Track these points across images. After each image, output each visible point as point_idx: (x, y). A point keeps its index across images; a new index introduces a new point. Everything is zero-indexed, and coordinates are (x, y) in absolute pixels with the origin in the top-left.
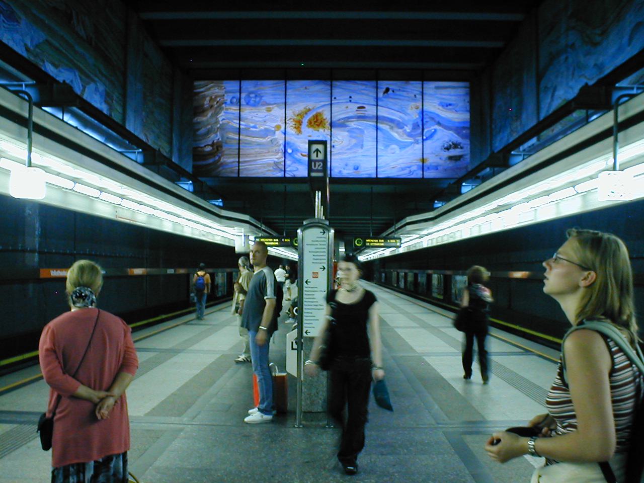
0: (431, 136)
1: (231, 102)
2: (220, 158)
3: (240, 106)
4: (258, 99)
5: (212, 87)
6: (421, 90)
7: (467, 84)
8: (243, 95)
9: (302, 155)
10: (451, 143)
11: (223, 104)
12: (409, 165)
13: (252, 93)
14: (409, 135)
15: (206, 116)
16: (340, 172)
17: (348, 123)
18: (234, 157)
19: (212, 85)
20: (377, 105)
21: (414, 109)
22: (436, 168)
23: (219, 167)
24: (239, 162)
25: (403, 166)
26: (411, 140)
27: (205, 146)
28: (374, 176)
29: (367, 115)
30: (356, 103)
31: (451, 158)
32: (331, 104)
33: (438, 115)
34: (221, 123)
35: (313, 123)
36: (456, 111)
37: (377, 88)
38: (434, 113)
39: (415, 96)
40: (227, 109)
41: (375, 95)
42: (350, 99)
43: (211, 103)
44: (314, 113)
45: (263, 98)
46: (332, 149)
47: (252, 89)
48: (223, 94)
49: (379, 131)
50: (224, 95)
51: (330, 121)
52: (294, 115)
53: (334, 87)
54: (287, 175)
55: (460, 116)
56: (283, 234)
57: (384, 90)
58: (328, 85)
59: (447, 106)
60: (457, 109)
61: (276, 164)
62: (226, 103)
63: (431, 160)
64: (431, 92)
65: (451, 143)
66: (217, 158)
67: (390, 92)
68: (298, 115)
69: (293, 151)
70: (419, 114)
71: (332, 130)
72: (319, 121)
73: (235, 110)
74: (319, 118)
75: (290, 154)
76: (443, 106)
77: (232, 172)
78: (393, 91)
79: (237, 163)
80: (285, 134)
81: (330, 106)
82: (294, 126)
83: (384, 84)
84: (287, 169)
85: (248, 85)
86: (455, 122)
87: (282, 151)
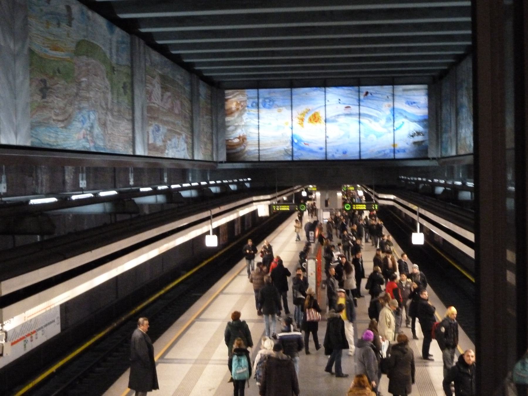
0: (400, 127)
1: (252, 106)
2: (245, 147)
3: (258, 108)
4: (271, 103)
5: (237, 95)
6: (392, 92)
7: (425, 86)
8: (261, 100)
9: (304, 144)
10: (415, 132)
11: (245, 107)
12: (384, 149)
13: (267, 98)
14: (385, 127)
15: (234, 116)
16: (333, 156)
17: (337, 119)
18: (256, 147)
19: (238, 93)
20: (359, 105)
21: (387, 107)
22: (404, 151)
23: (244, 154)
24: (259, 150)
25: (380, 150)
26: (385, 130)
27: (234, 139)
28: (358, 158)
29: (352, 113)
30: (344, 104)
31: (415, 143)
32: (325, 106)
33: (405, 111)
34: (245, 121)
35: (312, 119)
36: (418, 107)
37: (359, 92)
38: (402, 110)
39: (388, 97)
40: (249, 111)
41: (357, 98)
42: (340, 101)
43: (237, 107)
44: (313, 113)
45: (276, 103)
46: (327, 139)
47: (267, 96)
48: (245, 100)
49: (361, 124)
50: (246, 101)
51: (324, 119)
52: (299, 114)
53: (328, 93)
54: (295, 159)
55: (422, 111)
56: (292, 201)
57: (364, 93)
58: (322, 91)
59: (412, 104)
60: (419, 106)
61: (286, 151)
62: (248, 107)
63: (400, 145)
64: (400, 94)
65: (415, 132)
66: (243, 147)
67: (369, 95)
68: (301, 114)
69: (298, 141)
70: (390, 111)
71: (327, 124)
72: (317, 119)
73: (255, 111)
74: (317, 116)
75: (296, 144)
76: (409, 104)
77: (255, 158)
78: (371, 94)
79: (257, 151)
80: (292, 129)
81: (324, 107)
82: (299, 123)
83: (364, 89)
84: (295, 154)
85: (263, 92)
86: (417, 116)
87: (290, 141)
